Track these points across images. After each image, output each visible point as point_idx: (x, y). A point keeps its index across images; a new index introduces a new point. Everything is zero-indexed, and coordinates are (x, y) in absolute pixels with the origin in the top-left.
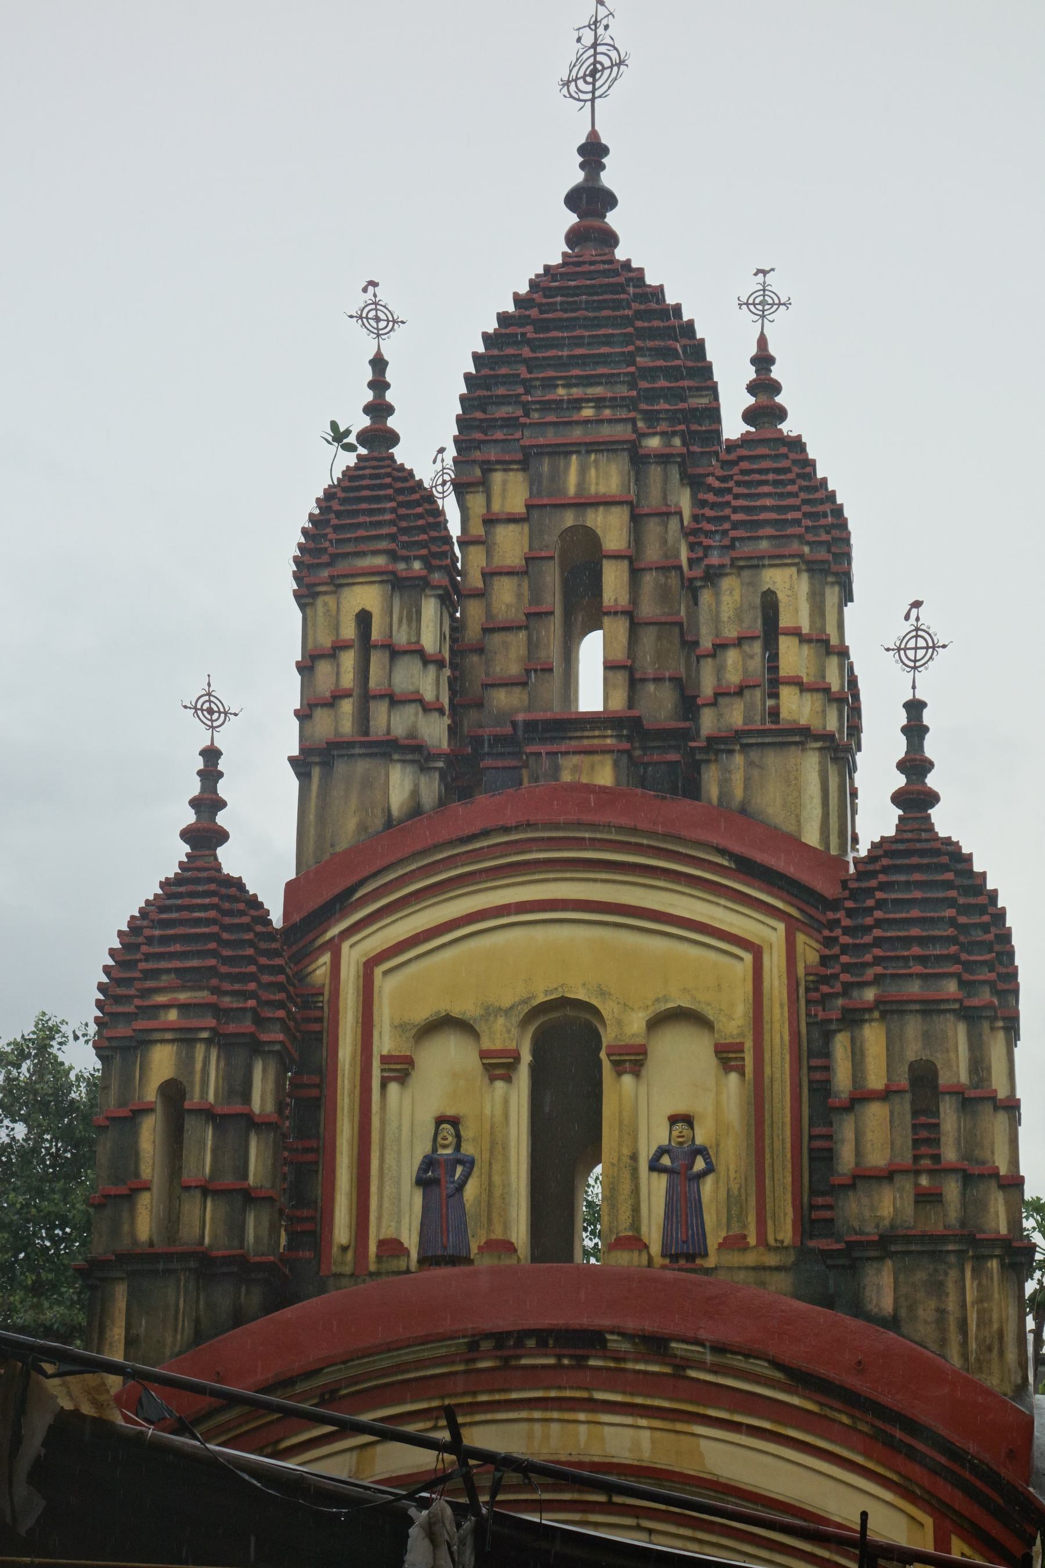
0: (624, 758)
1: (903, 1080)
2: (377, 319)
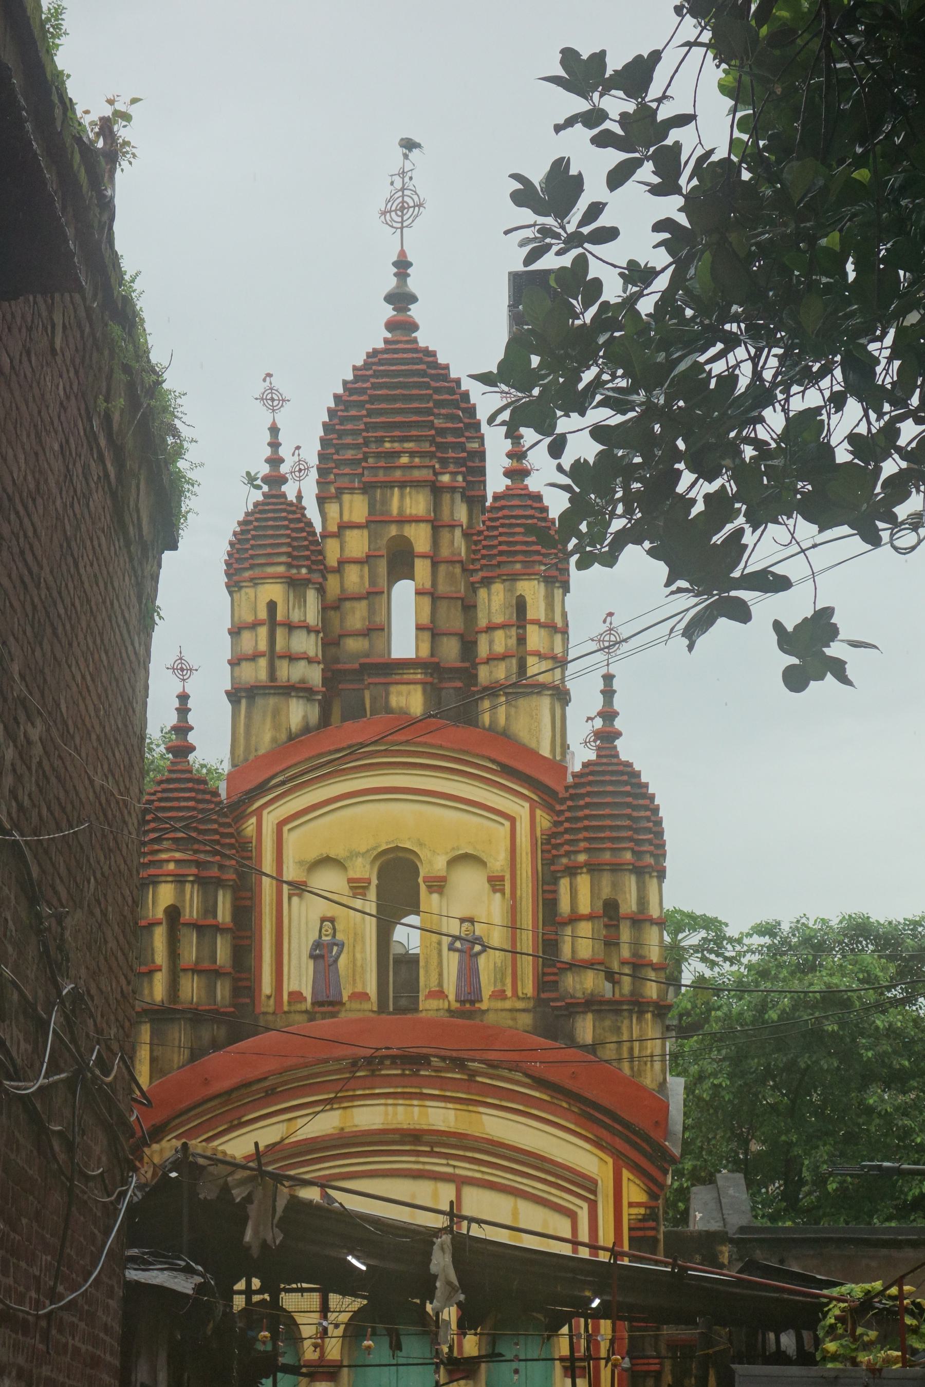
0: (428, 687)
1: (600, 904)
2: (273, 400)
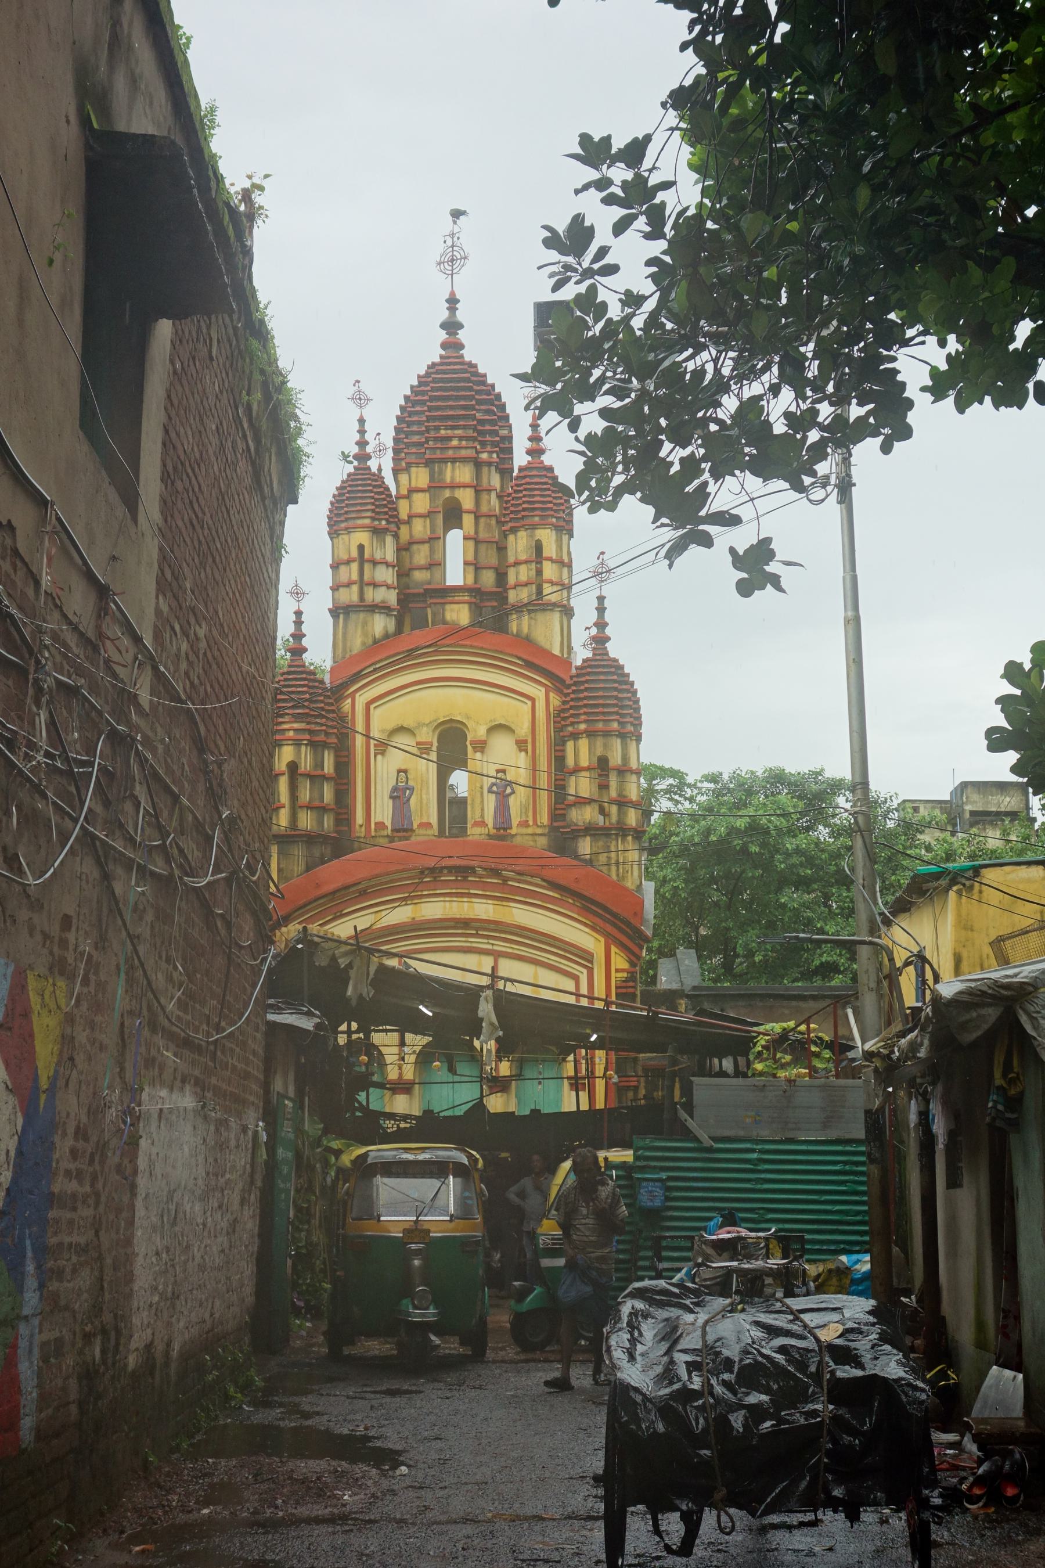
0: (473, 606)
1: (595, 760)
2: (360, 399)
